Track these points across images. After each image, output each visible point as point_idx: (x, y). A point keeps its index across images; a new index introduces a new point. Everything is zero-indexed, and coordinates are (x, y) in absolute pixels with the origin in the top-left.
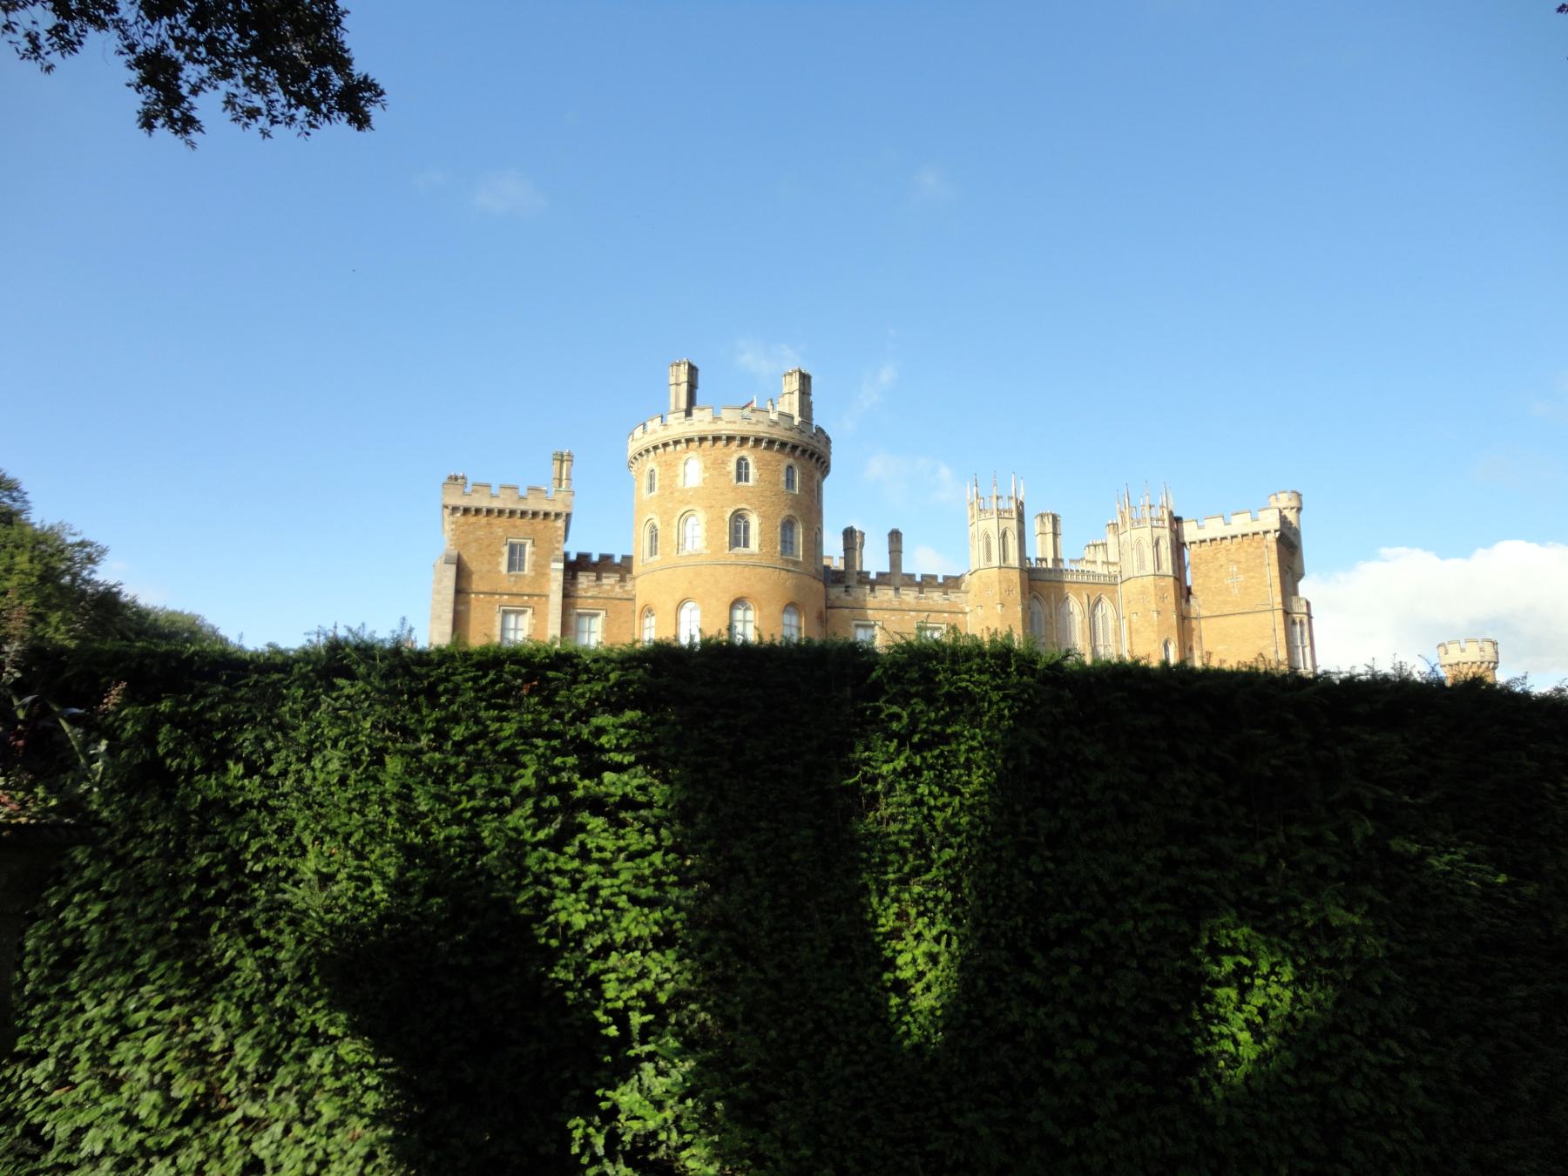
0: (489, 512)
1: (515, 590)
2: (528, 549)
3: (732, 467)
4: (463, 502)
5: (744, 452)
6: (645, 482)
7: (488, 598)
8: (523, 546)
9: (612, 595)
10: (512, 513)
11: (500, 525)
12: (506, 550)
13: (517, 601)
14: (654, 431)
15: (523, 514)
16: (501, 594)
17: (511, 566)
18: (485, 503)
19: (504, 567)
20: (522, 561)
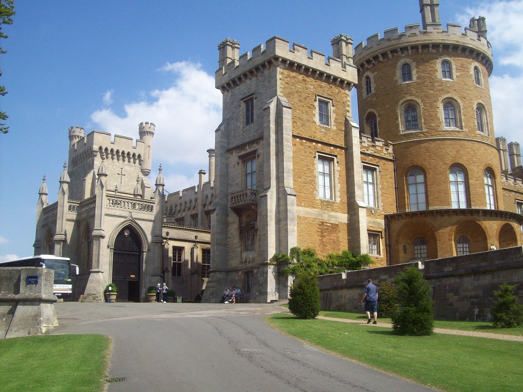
0: (307, 69)
1: (325, 140)
2: (331, 108)
3: (472, 72)
4: (290, 57)
5: (477, 64)
6: (399, 73)
7: (308, 144)
8: (327, 103)
9: (382, 155)
10: (322, 74)
11: (312, 84)
12: (317, 104)
13: (327, 149)
14: (414, 35)
15: (329, 76)
16: (317, 142)
17: (321, 120)
18: (305, 62)
19: (317, 119)
20: (327, 117)
